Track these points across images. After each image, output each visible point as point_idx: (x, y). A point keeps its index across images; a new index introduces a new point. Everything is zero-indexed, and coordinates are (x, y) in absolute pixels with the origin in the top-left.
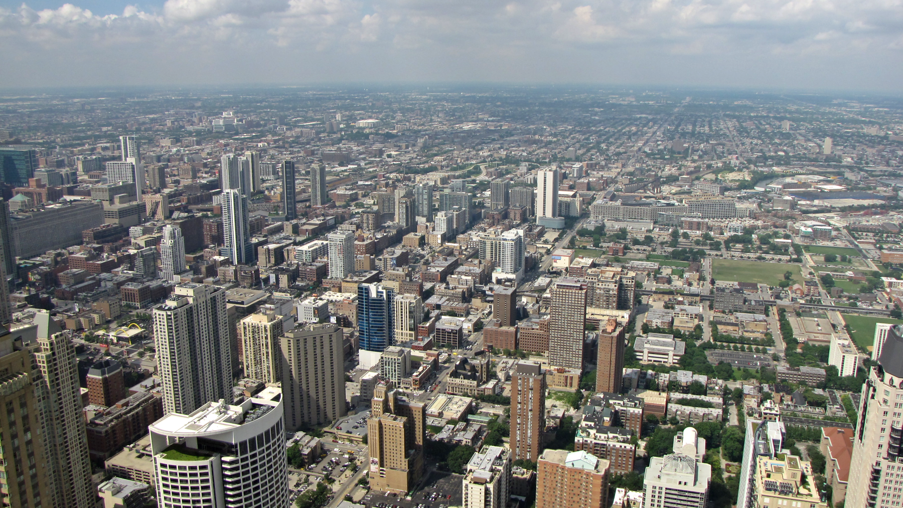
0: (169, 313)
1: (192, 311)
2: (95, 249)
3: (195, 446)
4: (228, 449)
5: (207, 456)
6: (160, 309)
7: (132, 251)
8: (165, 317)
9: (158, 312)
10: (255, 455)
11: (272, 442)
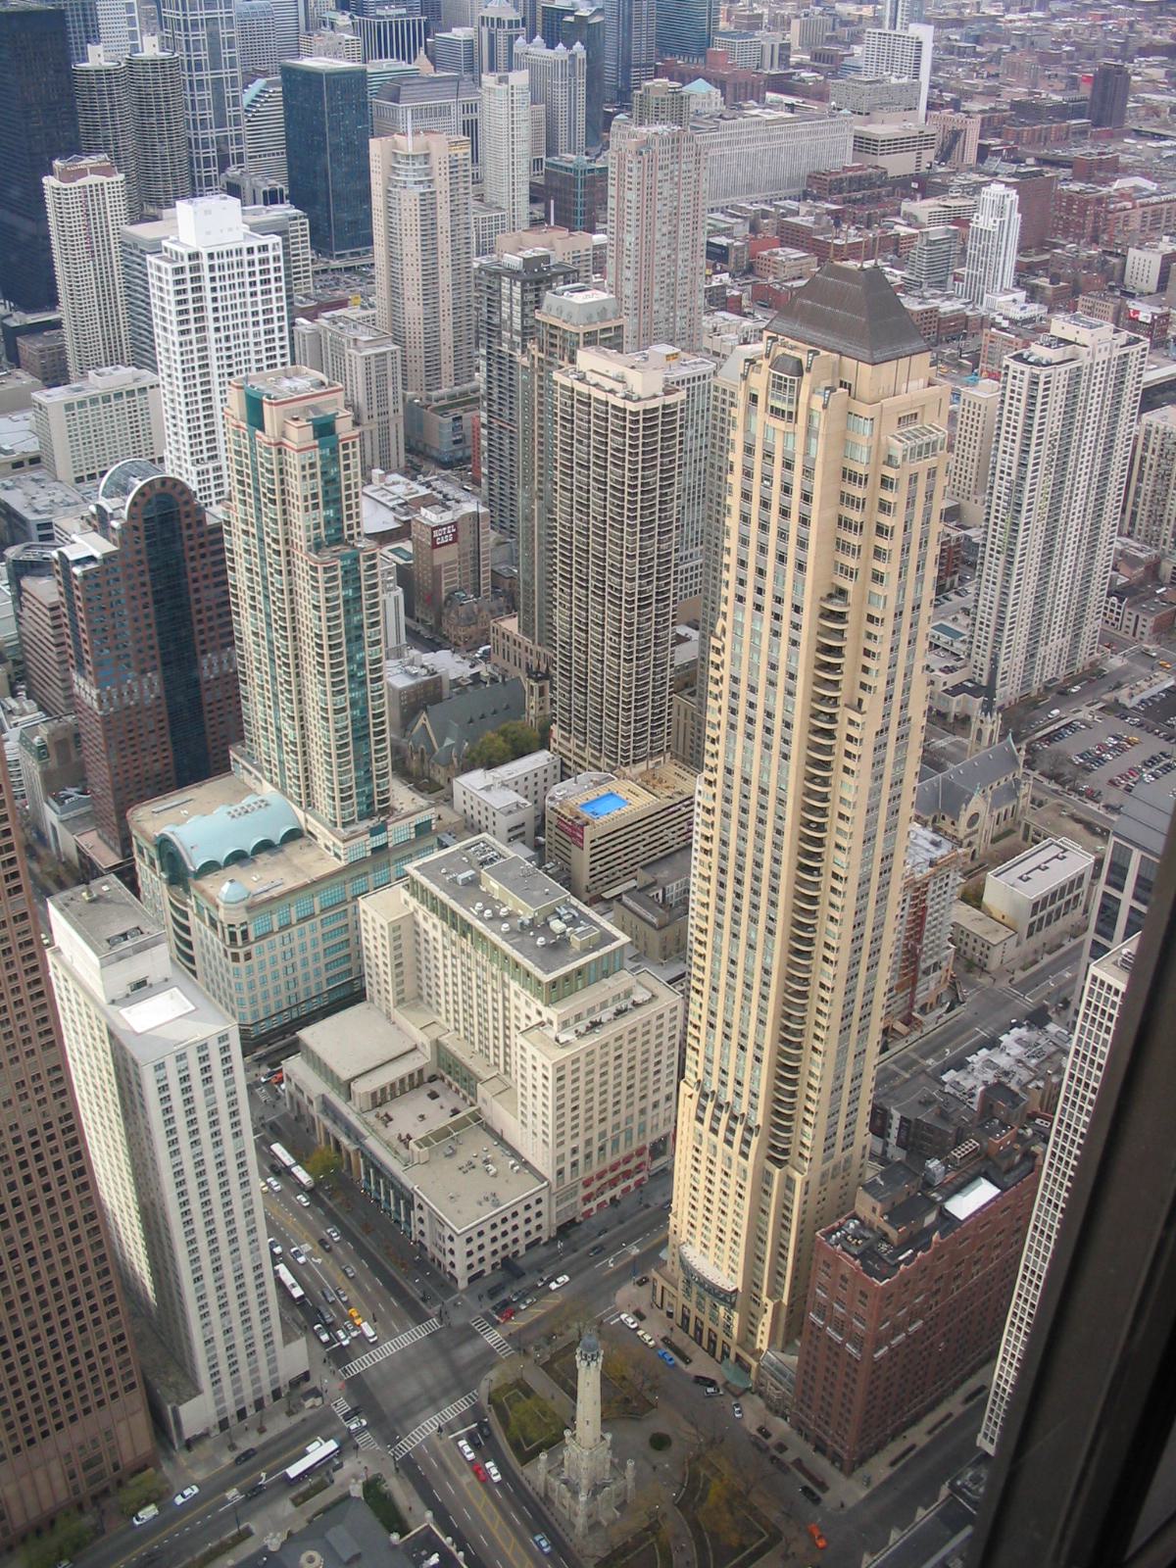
0: (1036, 370)
2: (829, 212)
6: (1019, 358)
7: (903, 230)
8: (1026, 378)
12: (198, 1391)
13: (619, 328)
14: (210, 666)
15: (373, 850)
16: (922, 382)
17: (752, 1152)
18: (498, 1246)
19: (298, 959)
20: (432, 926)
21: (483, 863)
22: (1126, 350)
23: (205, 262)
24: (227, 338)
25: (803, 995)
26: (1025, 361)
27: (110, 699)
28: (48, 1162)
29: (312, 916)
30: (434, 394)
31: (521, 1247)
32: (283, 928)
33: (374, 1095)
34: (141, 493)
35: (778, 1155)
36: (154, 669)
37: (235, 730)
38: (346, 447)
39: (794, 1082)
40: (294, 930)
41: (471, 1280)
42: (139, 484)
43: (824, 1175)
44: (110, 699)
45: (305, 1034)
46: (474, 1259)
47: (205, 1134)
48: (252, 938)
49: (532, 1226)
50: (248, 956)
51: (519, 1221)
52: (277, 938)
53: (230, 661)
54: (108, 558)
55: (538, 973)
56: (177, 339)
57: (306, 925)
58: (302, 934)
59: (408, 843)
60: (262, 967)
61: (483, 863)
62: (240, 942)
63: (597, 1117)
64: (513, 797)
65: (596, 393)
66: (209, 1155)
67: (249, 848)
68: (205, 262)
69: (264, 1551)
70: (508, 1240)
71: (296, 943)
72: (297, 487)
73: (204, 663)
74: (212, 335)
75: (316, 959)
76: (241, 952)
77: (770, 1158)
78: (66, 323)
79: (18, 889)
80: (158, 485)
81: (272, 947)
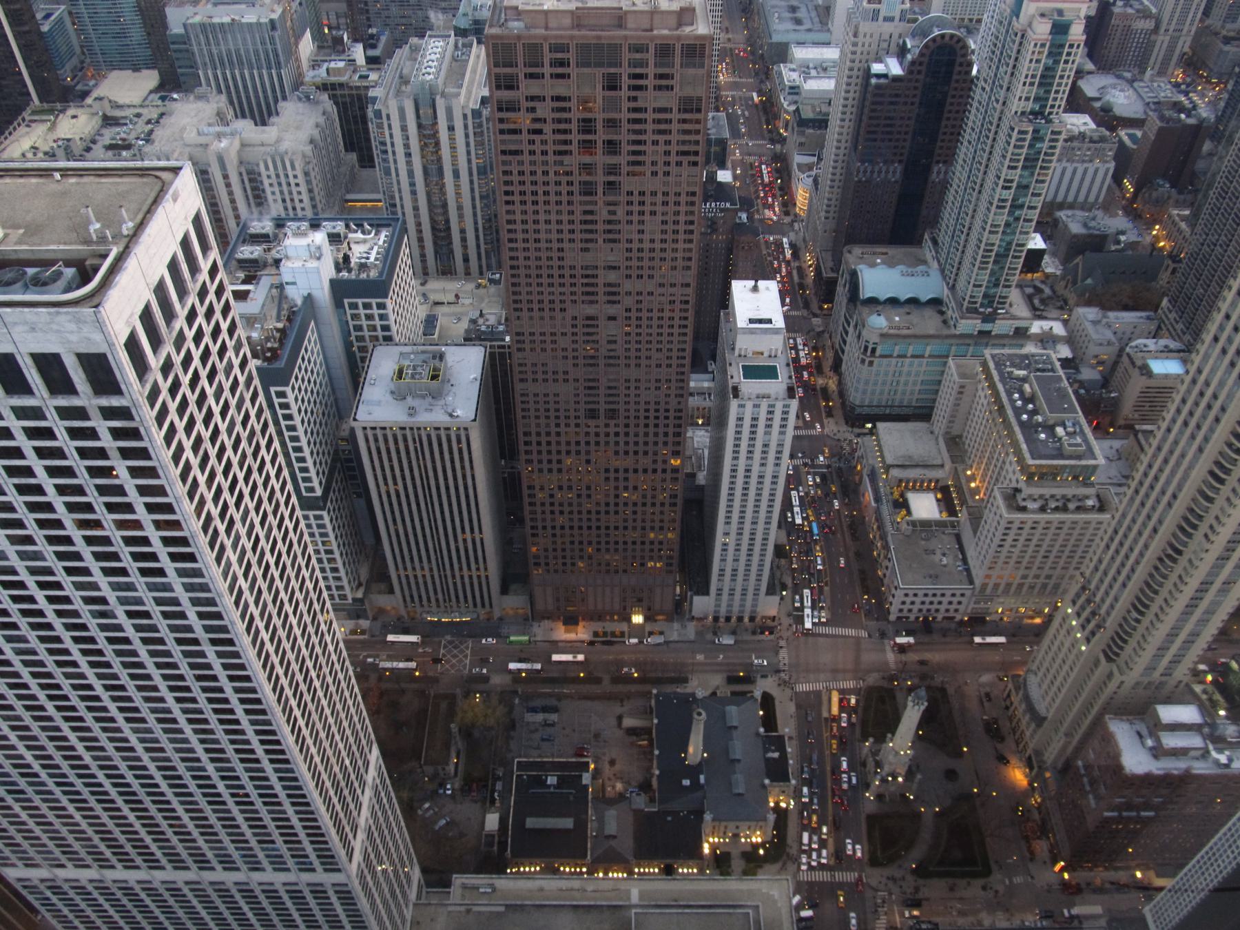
12: (707, 593)
14: (939, 173)
15: (980, 332)
17: (1094, 641)
18: (925, 607)
19: (902, 379)
20: (984, 394)
25: (1174, 561)
28: (661, 430)
30: (1228, 26)
31: (940, 617)
33: (900, 481)
34: (934, 40)
35: (1111, 653)
37: (934, 222)
38: (1071, 46)
39: (1142, 613)
40: (907, 361)
41: (899, 618)
42: (937, 32)
43: (1137, 683)
45: (880, 425)
46: (906, 607)
47: (757, 455)
48: (878, 353)
49: (952, 607)
50: (871, 363)
51: (945, 600)
52: (894, 361)
53: (946, 173)
54: (896, 79)
55: (1027, 455)
57: (916, 361)
58: (911, 365)
59: (1006, 336)
60: (877, 375)
63: (1024, 564)
64: (1109, 334)
66: (756, 469)
67: (903, 297)
69: (693, 695)
70: (933, 607)
71: (905, 369)
72: (1025, 67)
73: (935, 169)
75: (915, 384)
77: (1104, 651)
79: (688, 268)
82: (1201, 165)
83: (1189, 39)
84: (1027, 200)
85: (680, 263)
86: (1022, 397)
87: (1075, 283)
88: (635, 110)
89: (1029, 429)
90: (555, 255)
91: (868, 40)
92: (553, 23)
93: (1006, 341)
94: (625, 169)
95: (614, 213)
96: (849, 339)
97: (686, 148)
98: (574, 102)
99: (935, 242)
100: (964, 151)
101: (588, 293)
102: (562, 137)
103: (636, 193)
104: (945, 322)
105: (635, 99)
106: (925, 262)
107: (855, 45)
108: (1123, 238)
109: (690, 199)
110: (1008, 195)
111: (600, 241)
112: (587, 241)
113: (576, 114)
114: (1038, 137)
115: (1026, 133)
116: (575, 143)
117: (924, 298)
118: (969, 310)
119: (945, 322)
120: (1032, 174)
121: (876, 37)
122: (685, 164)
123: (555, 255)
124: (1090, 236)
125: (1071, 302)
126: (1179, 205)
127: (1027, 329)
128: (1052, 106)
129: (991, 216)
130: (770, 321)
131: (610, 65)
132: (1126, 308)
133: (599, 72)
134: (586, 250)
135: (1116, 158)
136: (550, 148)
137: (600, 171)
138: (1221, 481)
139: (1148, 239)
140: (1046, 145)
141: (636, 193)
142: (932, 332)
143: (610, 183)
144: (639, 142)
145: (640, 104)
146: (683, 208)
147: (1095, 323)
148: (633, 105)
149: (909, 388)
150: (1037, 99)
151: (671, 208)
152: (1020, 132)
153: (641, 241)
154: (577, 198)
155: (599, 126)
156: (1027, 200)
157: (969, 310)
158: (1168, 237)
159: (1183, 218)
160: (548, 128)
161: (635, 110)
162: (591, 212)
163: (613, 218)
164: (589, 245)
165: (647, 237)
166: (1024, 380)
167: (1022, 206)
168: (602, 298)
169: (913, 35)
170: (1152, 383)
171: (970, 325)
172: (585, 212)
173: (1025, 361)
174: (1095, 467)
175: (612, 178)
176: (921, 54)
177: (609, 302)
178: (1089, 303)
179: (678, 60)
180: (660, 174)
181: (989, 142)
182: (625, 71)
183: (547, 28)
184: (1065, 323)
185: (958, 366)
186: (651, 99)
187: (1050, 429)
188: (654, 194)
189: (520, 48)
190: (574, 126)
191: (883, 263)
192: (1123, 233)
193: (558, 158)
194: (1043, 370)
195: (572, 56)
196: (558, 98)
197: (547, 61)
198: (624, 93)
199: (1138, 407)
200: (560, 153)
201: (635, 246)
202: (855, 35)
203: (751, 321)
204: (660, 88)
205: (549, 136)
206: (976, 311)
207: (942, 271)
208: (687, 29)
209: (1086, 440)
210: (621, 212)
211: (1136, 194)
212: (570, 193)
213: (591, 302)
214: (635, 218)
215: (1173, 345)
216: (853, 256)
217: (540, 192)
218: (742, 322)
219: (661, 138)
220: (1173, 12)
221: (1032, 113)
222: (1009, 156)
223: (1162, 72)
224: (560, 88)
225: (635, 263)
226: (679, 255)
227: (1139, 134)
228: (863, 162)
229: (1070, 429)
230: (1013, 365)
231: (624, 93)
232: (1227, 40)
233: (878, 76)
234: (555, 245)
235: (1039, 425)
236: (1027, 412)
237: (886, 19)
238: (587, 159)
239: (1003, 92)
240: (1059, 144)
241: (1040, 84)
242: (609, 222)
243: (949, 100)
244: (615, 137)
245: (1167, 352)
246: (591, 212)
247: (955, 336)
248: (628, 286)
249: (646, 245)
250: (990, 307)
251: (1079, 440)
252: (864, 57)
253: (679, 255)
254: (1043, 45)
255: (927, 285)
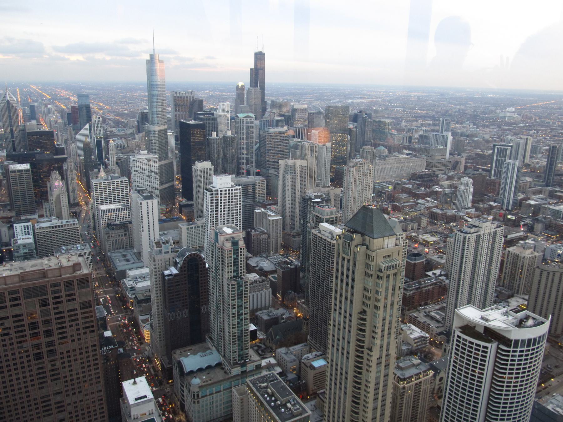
0: (465, 235)
1: (479, 237)
2: (417, 184)
3: (482, 331)
4: (506, 341)
5: (489, 341)
8: (462, 237)
9: (458, 233)
10: (522, 351)
11: (537, 346)
13: (336, 217)
14: (204, 309)
15: (241, 372)
16: (393, 244)
21: (271, 381)
22: (496, 230)
23: (219, 193)
24: (224, 214)
26: (462, 232)
27: (172, 316)
29: (220, 391)
30: (293, 232)
32: (210, 394)
34: (187, 257)
36: (187, 308)
37: (208, 330)
38: (241, 249)
40: (214, 395)
42: (188, 254)
44: (172, 316)
48: (200, 396)
50: (198, 402)
52: (208, 397)
53: (207, 308)
54: (176, 275)
56: (210, 213)
57: (218, 394)
58: (216, 397)
59: (253, 370)
60: (203, 407)
61: (271, 381)
62: (196, 397)
64: (293, 357)
65: (323, 237)
67: (204, 367)
68: (219, 193)
71: (215, 399)
72: (226, 261)
73: (202, 308)
74: (220, 213)
75: (220, 405)
76: (196, 401)
78: (195, 205)
79: (99, 382)
80: (192, 255)
81: (206, 400)
82: (302, 282)
83: (281, 239)
84: (243, 311)
85: (94, 381)
86: (269, 395)
87: (272, 339)
88: (58, 313)
89: (276, 408)
90: (24, 395)
91: (160, 262)
92: (8, 282)
93: (253, 373)
94: (57, 342)
95: (54, 365)
96: (185, 394)
97: (87, 325)
98: (25, 315)
99: (211, 339)
100: (212, 298)
101: (46, 411)
102: (21, 334)
103: (65, 352)
104: (225, 372)
105: (57, 308)
106: (209, 348)
107: (155, 265)
108: (284, 317)
109: (94, 348)
110: (235, 311)
111: (49, 381)
112: (41, 383)
113: (27, 321)
114: (239, 286)
115: (234, 285)
116: (28, 335)
117: (213, 364)
118: (234, 364)
119: (225, 372)
120: (242, 300)
121: (163, 260)
122: (88, 332)
123: (24, 395)
124: (272, 319)
125: (274, 348)
126: (300, 298)
127: (260, 365)
128: (241, 273)
129: (231, 321)
130: (145, 397)
131: (42, 295)
132: (296, 344)
133: (36, 300)
134: (42, 388)
135: (271, 287)
136: (14, 341)
137: (44, 346)
138: (358, 404)
139: (294, 314)
140: (244, 287)
141: (65, 352)
142: (221, 379)
143: (50, 351)
144: (63, 328)
145: (60, 310)
146: (91, 354)
147: (286, 354)
148: (56, 311)
149: (219, 408)
150: (234, 271)
151: (85, 355)
152: (232, 285)
153: (71, 375)
154: (33, 362)
155: (40, 325)
156: (243, 311)
157: (234, 364)
158: (300, 312)
159: (303, 303)
160: (12, 332)
161: (58, 313)
162: (42, 368)
163: (55, 367)
164: (44, 385)
165: (74, 372)
166: (267, 387)
167: (242, 314)
168: (54, 411)
169: (179, 257)
170: (316, 372)
171: (236, 370)
172: (38, 369)
173: (264, 379)
174: (309, 416)
175: (51, 348)
176: (184, 264)
177: (59, 412)
178: (281, 346)
179: (76, 287)
180: (76, 340)
181: (221, 292)
182: (50, 297)
183: (6, 285)
184: (274, 357)
185: (237, 391)
186: (65, 307)
187: (285, 406)
188: (74, 350)
189: (6, 293)
190: (26, 327)
191: (191, 354)
192: (284, 314)
193: (19, 345)
194: (273, 381)
195: (21, 295)
196: (16, 316)
197: (7, 300)
198: (51, 306)
199: (315, 384)
200: (20, 342)
201: (69, 379)
202: (154, 261)
203: (136, 399)
204: (69, 300)
205: (13, 335)
206: (237, 363)
207: (218, 350)
208: (78, 273)
209: (300, 406)
210: (58, 364)
211: (283, 298)
212: (29, 361)
213: (49, 415)
214: (66, 364)
215: (318, 353)
216: (177, 355)
217: (12, 364)
218: (131, 401)
219: (73, 323)
220: (273, 229)
221: (234, 277)
222: (230, 295)
223: (276, 252)
224: (16, 311)
225: (70, 387)
226: (93, 377)
227: (276, 276)
228: (171, 313)
229: (293, 403)
230: (260, 382)
231: (51, 306)
232: (294, 236)
233: (168, 275)
234: (24, 390)
235: (279, 405)
236: (273, 401)
237: (165, 253)
238: (36, 342)
239: (220, 271)
240: (249, 286)
241: (234, 265)
242: (53, 370)
243: (200, 279)
244: (50, 328)
245: (317, 357)
246: (42, 368)
247: (232, 377)
248: (68, 400)
249: (75, 377)
250: (242, 360)
251: (298, 406)
252: (160, 269)
253: (93, 377)
254: (230, 251)
255: (213, 358)
